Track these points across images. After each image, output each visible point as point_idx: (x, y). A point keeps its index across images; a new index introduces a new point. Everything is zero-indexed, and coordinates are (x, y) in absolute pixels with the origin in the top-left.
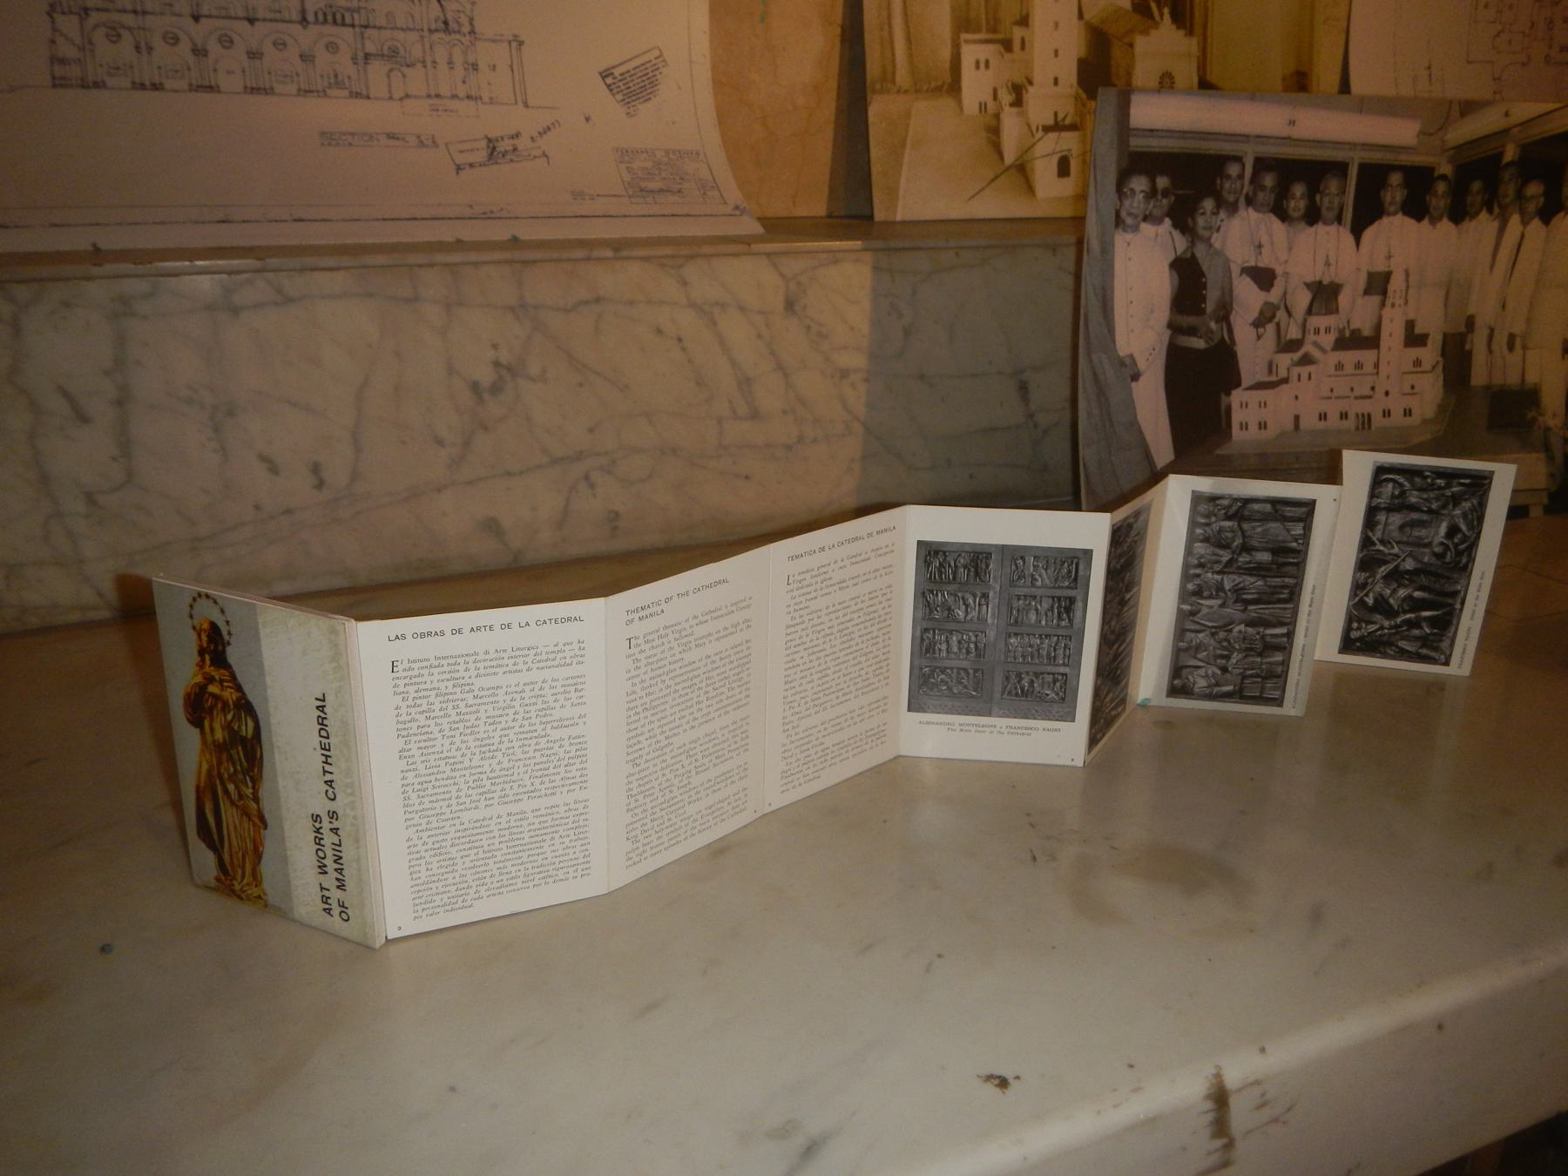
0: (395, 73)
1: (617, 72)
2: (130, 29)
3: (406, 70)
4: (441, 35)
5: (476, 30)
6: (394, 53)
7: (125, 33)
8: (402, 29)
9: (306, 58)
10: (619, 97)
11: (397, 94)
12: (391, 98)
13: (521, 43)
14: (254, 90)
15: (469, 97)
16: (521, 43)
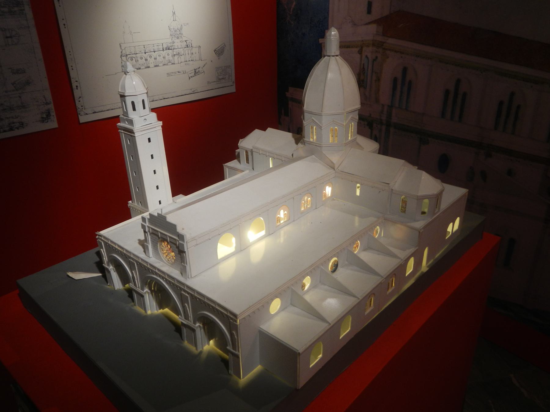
0: (179, 57)
1: (217, 50)
2: (134, 57)
3: (181, 57)
4: (186, 48)
5: (192, 46)
6: (179, 53)
7: (133, 58)
8: (180, 48)
9: (164, 58)
10: (217, 55)
11: (180, 62)
12: (178, 63)
13: (200, 47)
14: (156, 66)
15: (192, 60)
16: (200, 47)
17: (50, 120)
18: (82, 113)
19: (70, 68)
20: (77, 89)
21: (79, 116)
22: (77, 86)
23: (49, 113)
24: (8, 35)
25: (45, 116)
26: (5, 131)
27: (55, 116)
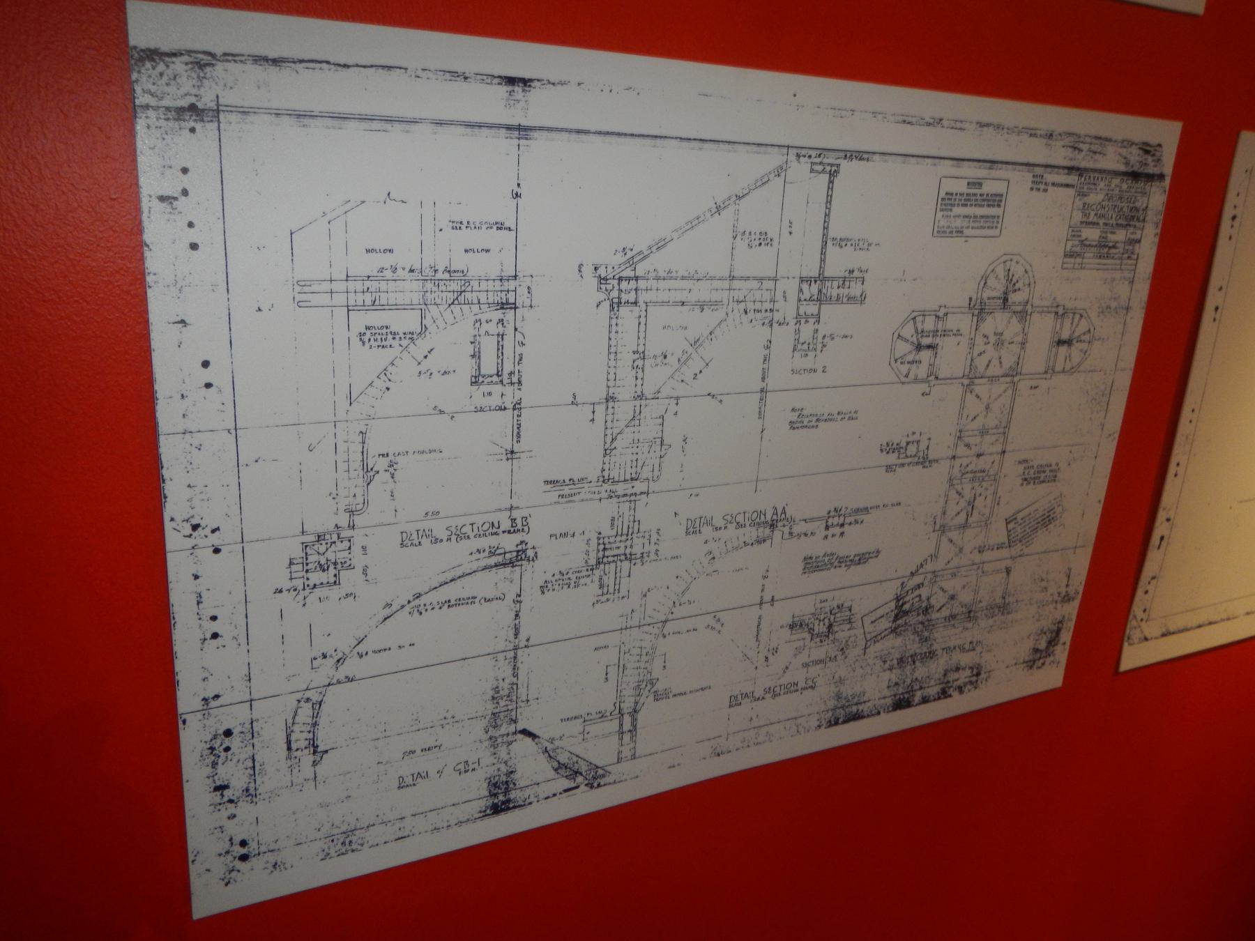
17: (1052, 658)
18: (1136, 635)
19: (1172, 469)
20: (1159, 547)
21: (1126, 644)
22: (1162, 538)
23: (1058, 632)
24: (1065, 335)
25: (1042, 645)
26: (925, 700)
27: (1067, 646)
